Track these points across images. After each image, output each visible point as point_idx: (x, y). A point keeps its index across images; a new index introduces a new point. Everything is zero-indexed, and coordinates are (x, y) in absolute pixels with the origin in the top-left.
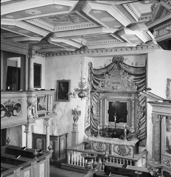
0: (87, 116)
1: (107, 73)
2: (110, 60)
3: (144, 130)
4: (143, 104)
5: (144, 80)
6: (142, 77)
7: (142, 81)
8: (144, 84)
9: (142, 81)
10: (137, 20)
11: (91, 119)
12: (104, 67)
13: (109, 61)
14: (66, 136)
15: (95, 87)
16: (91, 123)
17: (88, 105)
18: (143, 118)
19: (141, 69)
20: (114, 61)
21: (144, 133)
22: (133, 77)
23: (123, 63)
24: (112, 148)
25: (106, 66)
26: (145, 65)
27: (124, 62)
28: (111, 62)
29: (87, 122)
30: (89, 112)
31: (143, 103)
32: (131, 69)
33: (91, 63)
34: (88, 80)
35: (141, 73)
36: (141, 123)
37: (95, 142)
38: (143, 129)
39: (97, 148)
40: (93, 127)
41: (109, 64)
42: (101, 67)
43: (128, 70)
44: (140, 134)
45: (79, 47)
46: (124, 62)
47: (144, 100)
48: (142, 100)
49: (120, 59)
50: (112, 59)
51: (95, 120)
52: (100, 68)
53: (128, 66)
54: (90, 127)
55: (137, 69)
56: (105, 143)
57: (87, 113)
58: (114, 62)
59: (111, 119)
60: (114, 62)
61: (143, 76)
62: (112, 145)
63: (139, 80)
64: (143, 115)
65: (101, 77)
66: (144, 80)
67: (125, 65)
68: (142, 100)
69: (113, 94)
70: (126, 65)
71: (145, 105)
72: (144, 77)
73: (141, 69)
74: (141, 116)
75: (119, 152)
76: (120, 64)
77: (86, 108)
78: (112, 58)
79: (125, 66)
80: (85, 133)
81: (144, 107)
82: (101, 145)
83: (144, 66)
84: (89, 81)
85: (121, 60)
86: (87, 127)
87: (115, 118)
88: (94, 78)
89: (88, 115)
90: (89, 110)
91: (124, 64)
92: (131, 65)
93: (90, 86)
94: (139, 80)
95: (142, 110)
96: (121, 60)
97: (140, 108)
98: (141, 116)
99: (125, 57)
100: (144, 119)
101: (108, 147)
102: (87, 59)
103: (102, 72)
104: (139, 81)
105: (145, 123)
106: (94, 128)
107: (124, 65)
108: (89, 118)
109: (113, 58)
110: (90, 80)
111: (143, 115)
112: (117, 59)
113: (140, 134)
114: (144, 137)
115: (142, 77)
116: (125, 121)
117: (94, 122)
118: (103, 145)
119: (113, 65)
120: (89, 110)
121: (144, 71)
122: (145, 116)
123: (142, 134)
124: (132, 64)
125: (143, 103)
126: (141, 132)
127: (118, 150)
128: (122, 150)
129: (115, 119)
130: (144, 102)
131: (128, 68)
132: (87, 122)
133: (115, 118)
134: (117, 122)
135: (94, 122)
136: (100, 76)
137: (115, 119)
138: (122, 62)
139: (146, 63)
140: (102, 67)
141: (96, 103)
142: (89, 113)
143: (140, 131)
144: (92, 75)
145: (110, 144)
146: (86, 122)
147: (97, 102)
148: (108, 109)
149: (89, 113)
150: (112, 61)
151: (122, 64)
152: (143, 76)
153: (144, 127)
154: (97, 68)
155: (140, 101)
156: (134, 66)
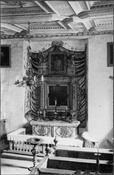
0: (27, 101)
3: (84, 112)
6: (82, 61)
8: (83, 68)
10: (89, 9)
11: (30, 103)
14: (5, 122)
16: (30, 107)
17: (28, 89)
18: (83, 101)
19: (81, 53)
21: (84, 114)
23: (63, 47)
24: (54, 132)
25: (46, 50)
26: (84, 49)
28: (50, 47)
29: (27, 107)
36: (82, 106)
37: (37, 126)
38: (82, 111)
39: (38, 131)
41: (49, 48)
45: (19, 31)
47: (84, 83)
49: (59, 43)
50: (51, 43)
51: (35, 104)
54: (30, 111)
56: (47, 126)
57: (26, 98)
58: (53, 47)
59: (52, 103)
62: (55, 128)
63: (78, 64)
64: (84, 98)
68: (81, 84)
69: (53, 78)
71: (85, 88)
73: (81, 53)
75: (61, 134)
76: (60, 48)
77: (26, 93)
78: (51, 43)
80: (26, 117)
81: (84, 90)
82: (43, 128)
85: (60, 44)
86: (27, 112)
87: (56, 101)
88: (33, 62)
89: (28, 100)
90: (28, 94)
91: (64, 48)
94: (78, 64)
96: (60, 44)
97: (80, 91)
99: (64, 42)
101: (50, 130)
102: (26, 44)
104: (79, 65)
105: (85, 105)
106: (34, 112)
108: (29, 103)
111: (84, 98)
112: (57, 43)
114: (84, 119)
115: (82, 61)
116: (66, 105)
118: (44, 128)
120: (28, 94)
121: (84, 56)
122: (85, 99)
123: (82, 116)
126: (81, 114)
127: (60, 132)
128: (64, 133)
129: (56, 103)
130: (84, 85)
132: (27, 107)
133: (56, 101)
134: (58, 105)
137: (56, 103)
138: (62, 46)
139: (86, 48)
143: (81, 113)
145: (52, 127)
146: (26, 106)
148: (48, 92)
149: (28, 96)
150: (51, 45)
155: (80, 83)
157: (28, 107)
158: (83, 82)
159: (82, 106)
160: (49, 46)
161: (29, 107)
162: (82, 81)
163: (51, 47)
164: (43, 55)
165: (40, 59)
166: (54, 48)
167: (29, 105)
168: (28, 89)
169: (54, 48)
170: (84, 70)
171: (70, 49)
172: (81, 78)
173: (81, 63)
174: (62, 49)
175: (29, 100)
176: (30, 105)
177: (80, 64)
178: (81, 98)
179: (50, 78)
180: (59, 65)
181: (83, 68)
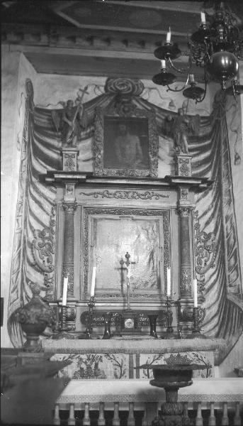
2: (97, 87)
4: (208, 226)
5: (208, 154)
6: (203, 144)
7: (203, 156)
9: (203, 156)
18: (211, 271)
20: (111, 88)
21: (213, 318)
23: (143, 100)
27: (145, 97)
28: (99, 93)
31: (207, 223)
33: (31, 82)
36: (206, 287)
41: (94, 96)
44: (204, 323)
47: (210, 214)
48: (205, 213)
49: (130, 85)
50: (104, 84)
58: (111, 94)
60: (111, 94)
61: (206, 143)
63: (195, 153)
66: (208, 154)
68: (205, 213)
69: (112, 191)
72: (210, 144)
74: (208, 263)
82: (97, 365)
83: (208, 115)
84: (26, 142)
89: (17, 265)
91: (146, 101)
95: (209, 243)
97: (202, 237)
98: (208, 263)
100: (213, 274)
112: (123, 85)
113: (204, 323)
115: (203, 144)
119: (109, 101)
120: (20, 246)
123: (209, 322)
124: (171, 104)
125: (207, 223)
132: (14, 290)
138: (138, 96)
142: (19, 257)
147: (47, 224)
150: (102, 89)
151: (138, 102)
152: (206, 143)
153: (215, 298)
154: (49, 108)
155: (200, 214)
157: (17, 291)
158: (209, 209)
159: (206, 287)
160: (97, 90)
161: (19, 293)
162: (205, 208)
163: (103, 95)
164: (81, 114)
165: (70, 123)
166: (112, 98)
167: (19, 287)
169: (112, 98)
171: (166, 107)
172: (204, 196)
173: (202, 150)
174: (138, 105)
176: (21, 288)
177: (198, 155)
178: (206, 261)
179: (101, 190)
180: (134, 151)
181: (207, 166)
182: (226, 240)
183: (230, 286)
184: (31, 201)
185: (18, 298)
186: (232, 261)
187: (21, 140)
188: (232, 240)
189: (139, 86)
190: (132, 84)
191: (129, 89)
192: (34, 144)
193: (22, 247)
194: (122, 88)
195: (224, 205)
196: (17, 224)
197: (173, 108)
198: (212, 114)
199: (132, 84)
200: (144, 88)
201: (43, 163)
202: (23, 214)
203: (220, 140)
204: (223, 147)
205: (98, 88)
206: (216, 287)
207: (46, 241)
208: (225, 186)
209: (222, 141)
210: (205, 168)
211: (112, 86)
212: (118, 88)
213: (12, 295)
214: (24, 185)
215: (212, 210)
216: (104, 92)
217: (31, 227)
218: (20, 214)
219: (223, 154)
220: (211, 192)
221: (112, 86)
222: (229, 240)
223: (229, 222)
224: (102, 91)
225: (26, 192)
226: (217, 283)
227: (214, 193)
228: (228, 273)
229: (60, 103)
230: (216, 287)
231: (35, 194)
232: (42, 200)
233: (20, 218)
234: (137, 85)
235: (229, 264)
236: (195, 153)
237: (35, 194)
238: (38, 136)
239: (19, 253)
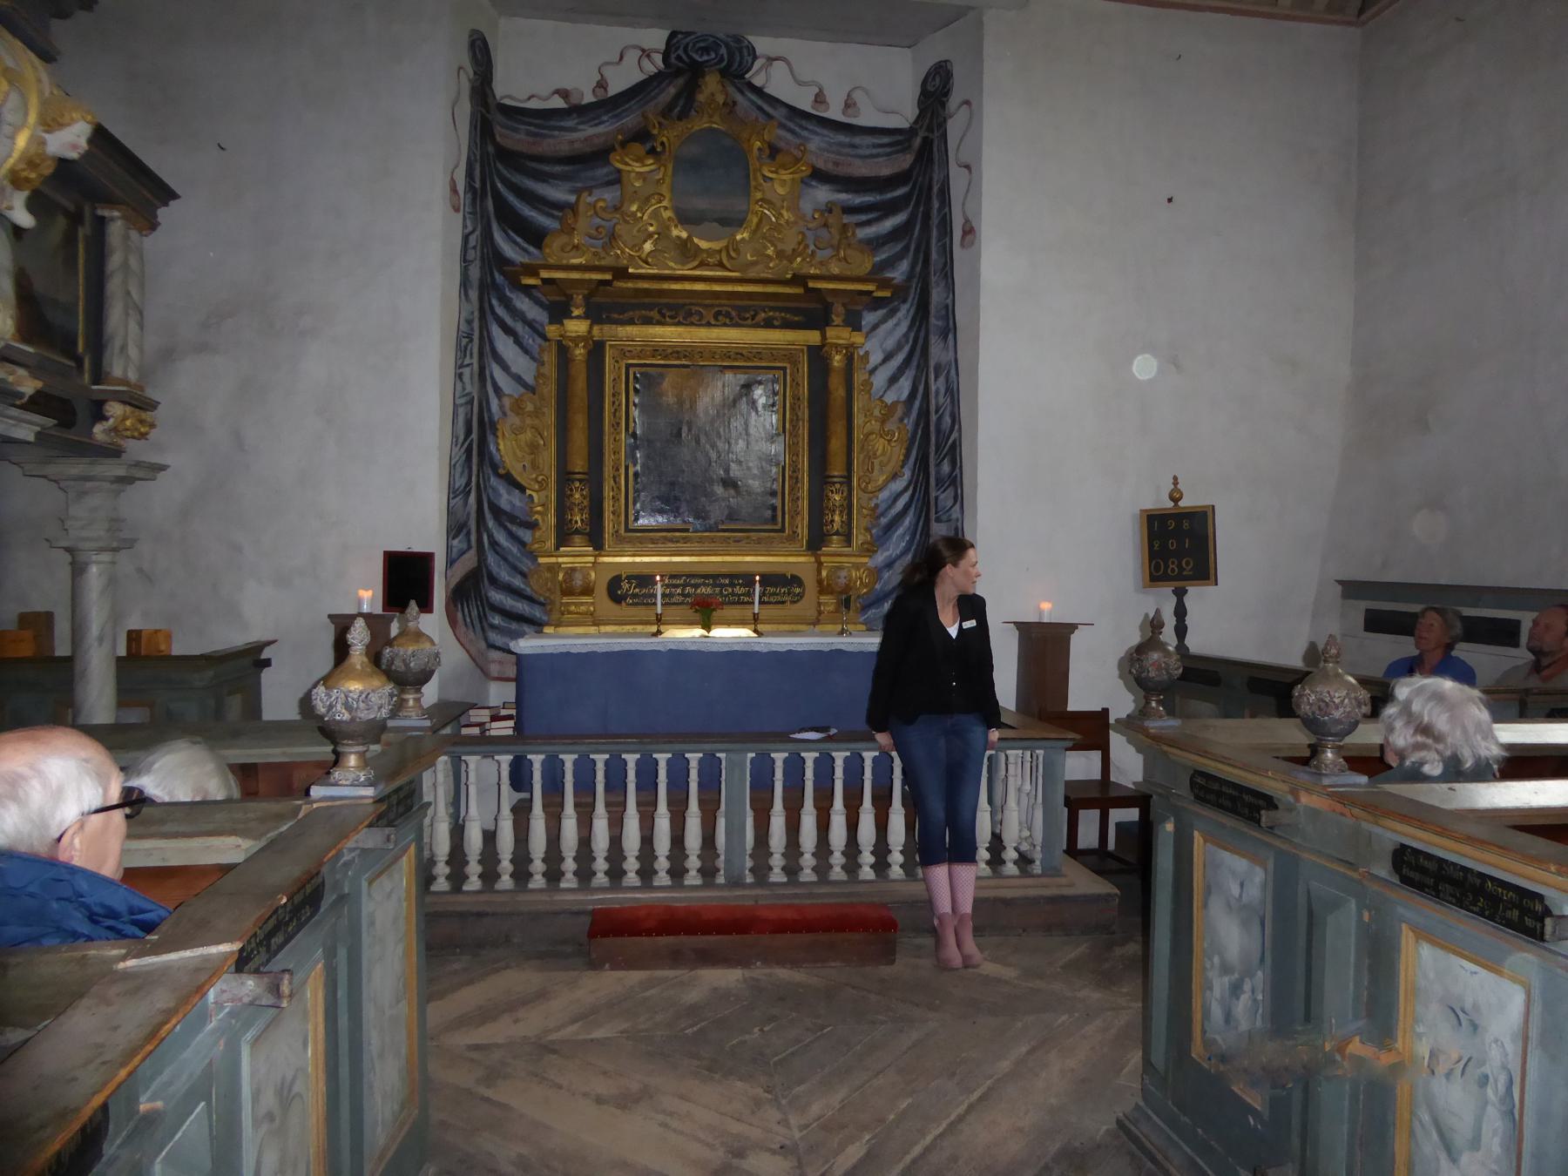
0: (460, 482)
1: (641, 135)
2: (647, 54)
4: (896, 386)
6: (889, 196)
7: (889, 224)
8: (899, 247)
9: (889, 224)
12: (589, 98)
13: (632, 57)
15: (509, 251)
17: (469, 388)
18: (898, 485)
20: (679, 58)
22: (823, 194)
28: (650, 69)
30: (471, 445)
31: (893, 380)
32: (805, 133)
34: (470, 174)
35: (886, 171)
36: (884, 521)
40: (494, 581)
41: (642, 77)
42: (564, 94)
43: (789, 136)
46: (757, 82)
47: (900, 358)
48: (888, 358)
49: (723, 51)
50: (663, 47)
51: (513, 519)
52: (558, 103)
53: (784, 111)
55: (857, 140)
58: (678, 73)
63: (870, 216)
65: (564, 177)
67: (760, 102)
70: (775, 101)
72: (906, 198)
73: (886, 140)
79: (760, 108)
83: (906, 125)
85: (731, 55)
88: (505, 181)
91: (759, 91)
92: (805, 104)
93: (478, 233)
94: (864, 218)
95: (891, 425)
99: (763, 44)
103: (575, 135)
104: (868, 223)
107: (754, 98)
108: (472, 498)
109: (673, 35)
110: (478, 185)
112: (706, 50)
115: (889, 196)
117: (501, 538)
119: (672, 90)
120: (468, 432)
124: (820, 99)
125: (893, 380)
131: (791, 125)
135: (501, 538)
136: (558, 169)
140: (574, 100)
141: (518, 379)
142: (469, 451)
144: (491, 149)
147: (529, 379)
150: (658, 58)
151: (742, 93)
154: (534, 104)
156: (834, 113)
157: (468, 534)
158: (899, 347)
160: (645, 62)
161: (473, 538)
162: (890, 343)
166: (681, 81)
168: (469, 388)
170: (904, 266)
172: (884, 320)
173: (888, 209)
175: (473, 483)
182: (933, 418)
183: (938, 520)
184: (496, 330)
185: (469, 547)
186: (946, 467)
187: (461, 187)
188: (947, 420)
189: (745, 52)
190: (727, 45)
191: (722, 59)
192: (497, 197)
193: (474, 436)
194: (705, 58)
195: (933, 339)
196: (459, 385)
197: (823, 107)
198: (916, 122)
199: (727, 45)
200: (755, 58)
201: (519, 240)
202: (475, 361)
203: (930, 188)
204: (936, 204)
205: (648, 56)
206: (907, 521)
207: (528, 421)
208: (937, 296)
209: (935, 189)
210: (892, 252)
211: (680, 52)
212: (696, 57)
213: (455, 542)
214: (474, 294)
215: (907, 349)
216: (662, 66)
217: (497, 390)
218: (467, 361)
219: (935, 221)
220: (904, 308)
221: (680, 52)
222: (939, 419)
223: (942, 379)
224: (655, 64)
225: (482, 309)
226: (911, 512)
227: (912, 311)
228: (933, 494)
229: (557, 92)
230: (907, 521)
231: (500, 311)
232: (519, 327)
233: (466, 371)
234: (740, 50)
235: (938, 472)
236: (870, 216)
237: (500, 311)
238: (505, 172)
239: (471, 445)
